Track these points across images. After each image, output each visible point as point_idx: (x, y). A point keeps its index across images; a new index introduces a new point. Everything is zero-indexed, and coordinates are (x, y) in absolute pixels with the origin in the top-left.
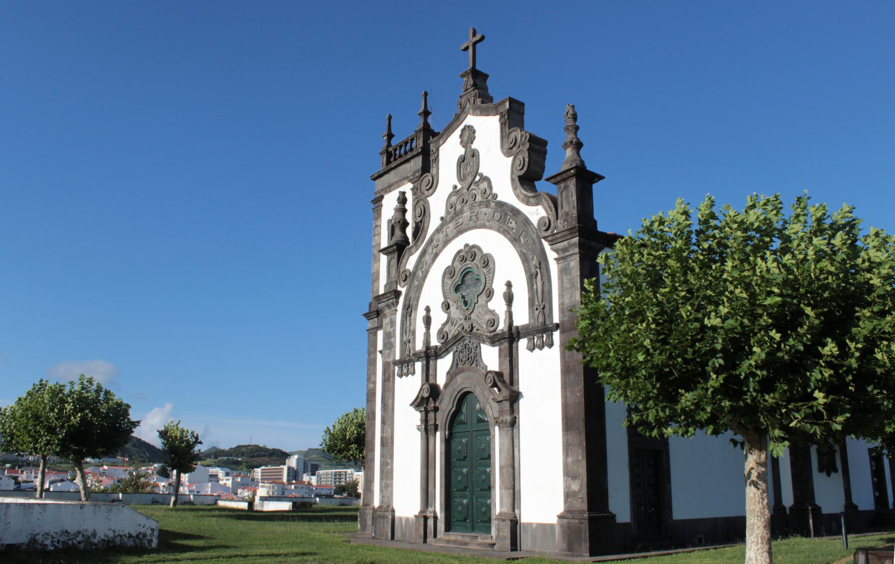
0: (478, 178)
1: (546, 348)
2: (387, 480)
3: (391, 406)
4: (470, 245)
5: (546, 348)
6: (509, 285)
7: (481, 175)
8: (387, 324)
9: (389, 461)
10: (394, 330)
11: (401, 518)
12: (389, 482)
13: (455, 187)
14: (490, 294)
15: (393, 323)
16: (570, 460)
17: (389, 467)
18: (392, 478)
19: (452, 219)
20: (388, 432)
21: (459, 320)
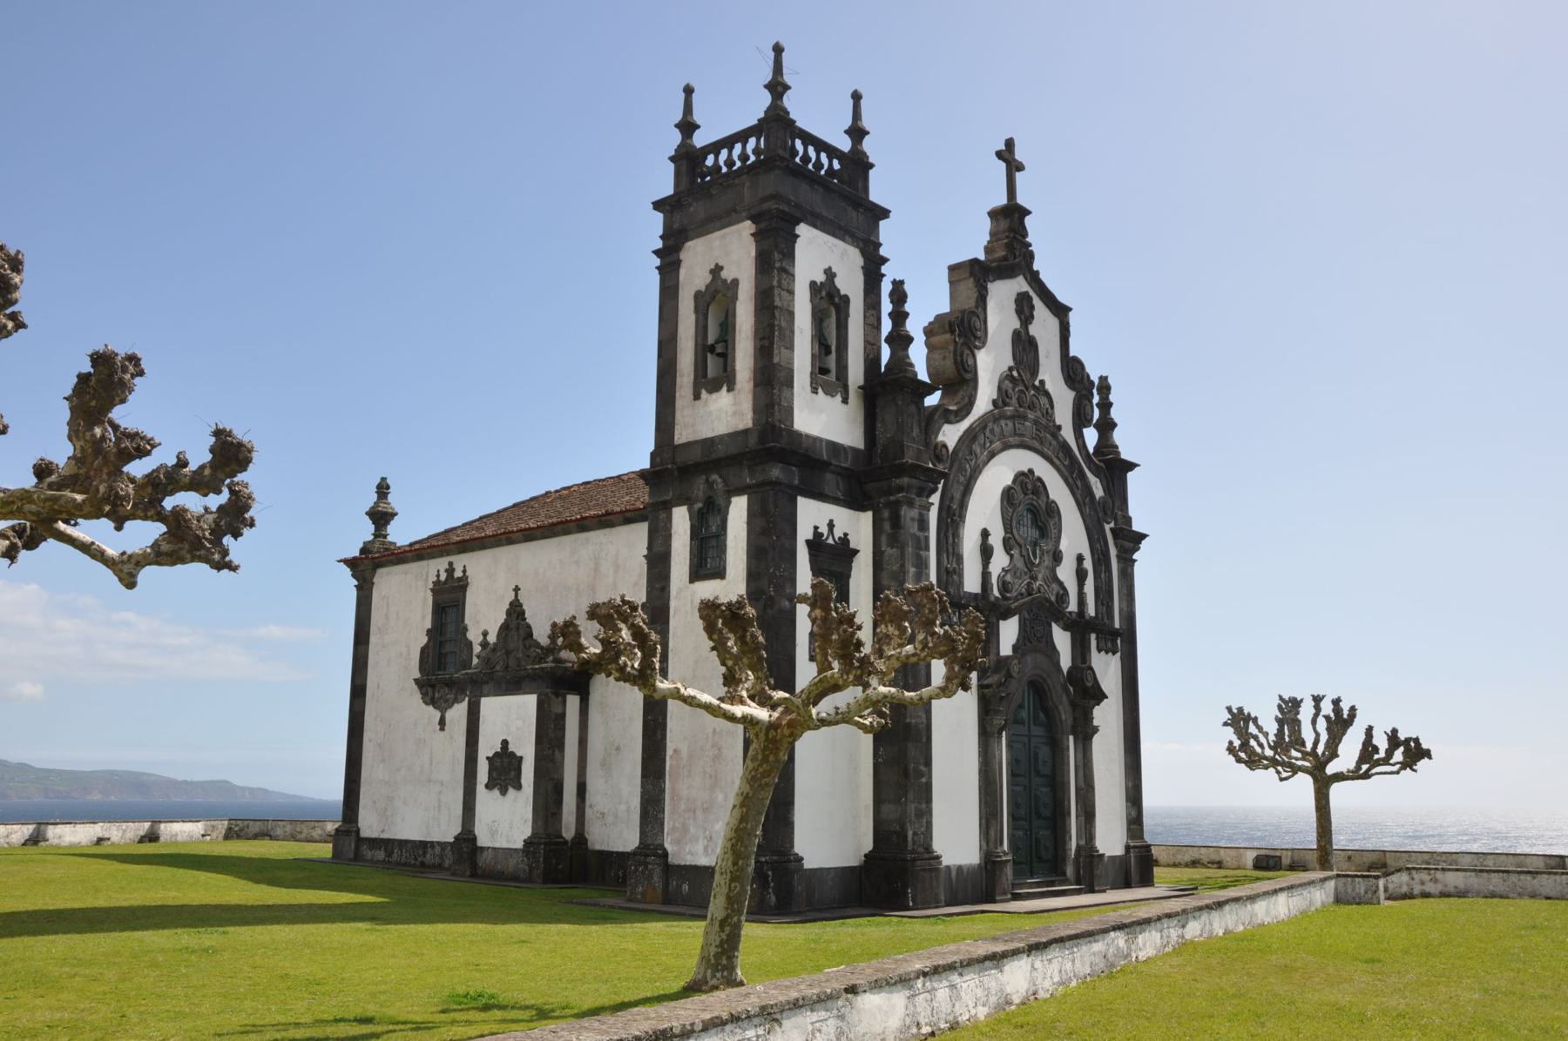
0: (1037, 383)
1: (1110, 654)
2: (920, 803)
3: (923, 672)
4: (1036, 474)
5: (1110, 654)
6: (985, 534)
7: (1042, 382)
8: (913, 519)
9: (923, 768)
10: (927, 539)
11: (948, 867)
12: (924, 806)
13: (1010, 369)
14: (1057, 558)
15: (923, 524)
16: (1130, 784)
17: (924, 780)
18: (929, 800)
19: (1012, 417)
20: (920, 717)
21: (1023, 574)
